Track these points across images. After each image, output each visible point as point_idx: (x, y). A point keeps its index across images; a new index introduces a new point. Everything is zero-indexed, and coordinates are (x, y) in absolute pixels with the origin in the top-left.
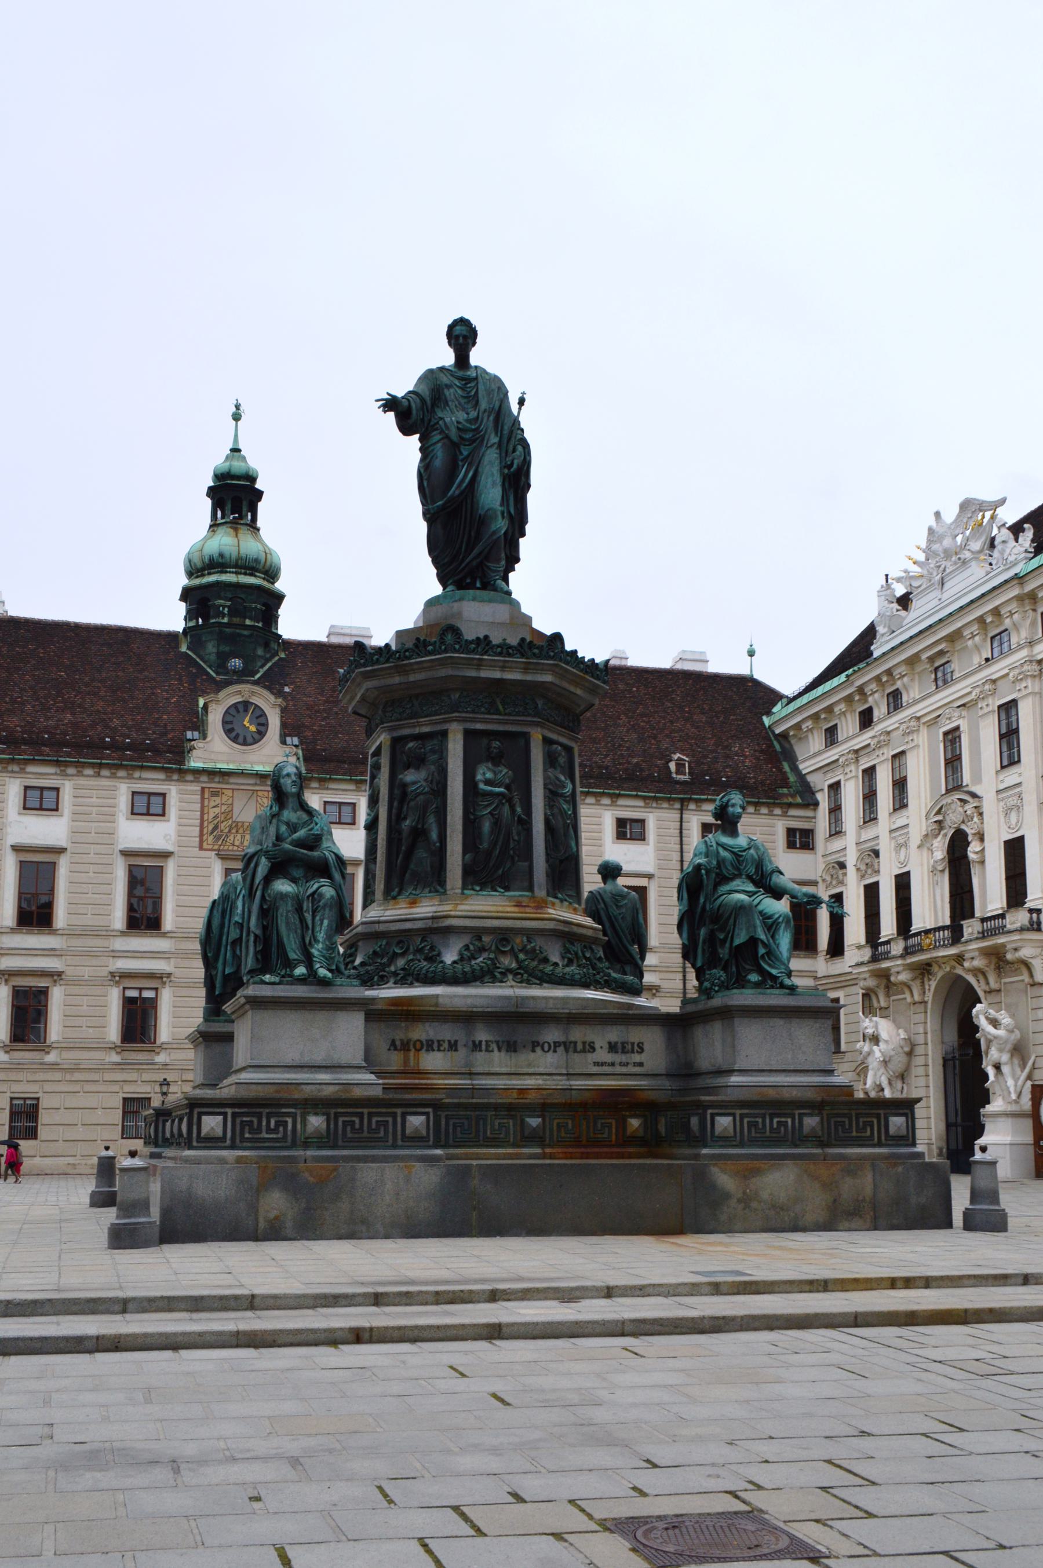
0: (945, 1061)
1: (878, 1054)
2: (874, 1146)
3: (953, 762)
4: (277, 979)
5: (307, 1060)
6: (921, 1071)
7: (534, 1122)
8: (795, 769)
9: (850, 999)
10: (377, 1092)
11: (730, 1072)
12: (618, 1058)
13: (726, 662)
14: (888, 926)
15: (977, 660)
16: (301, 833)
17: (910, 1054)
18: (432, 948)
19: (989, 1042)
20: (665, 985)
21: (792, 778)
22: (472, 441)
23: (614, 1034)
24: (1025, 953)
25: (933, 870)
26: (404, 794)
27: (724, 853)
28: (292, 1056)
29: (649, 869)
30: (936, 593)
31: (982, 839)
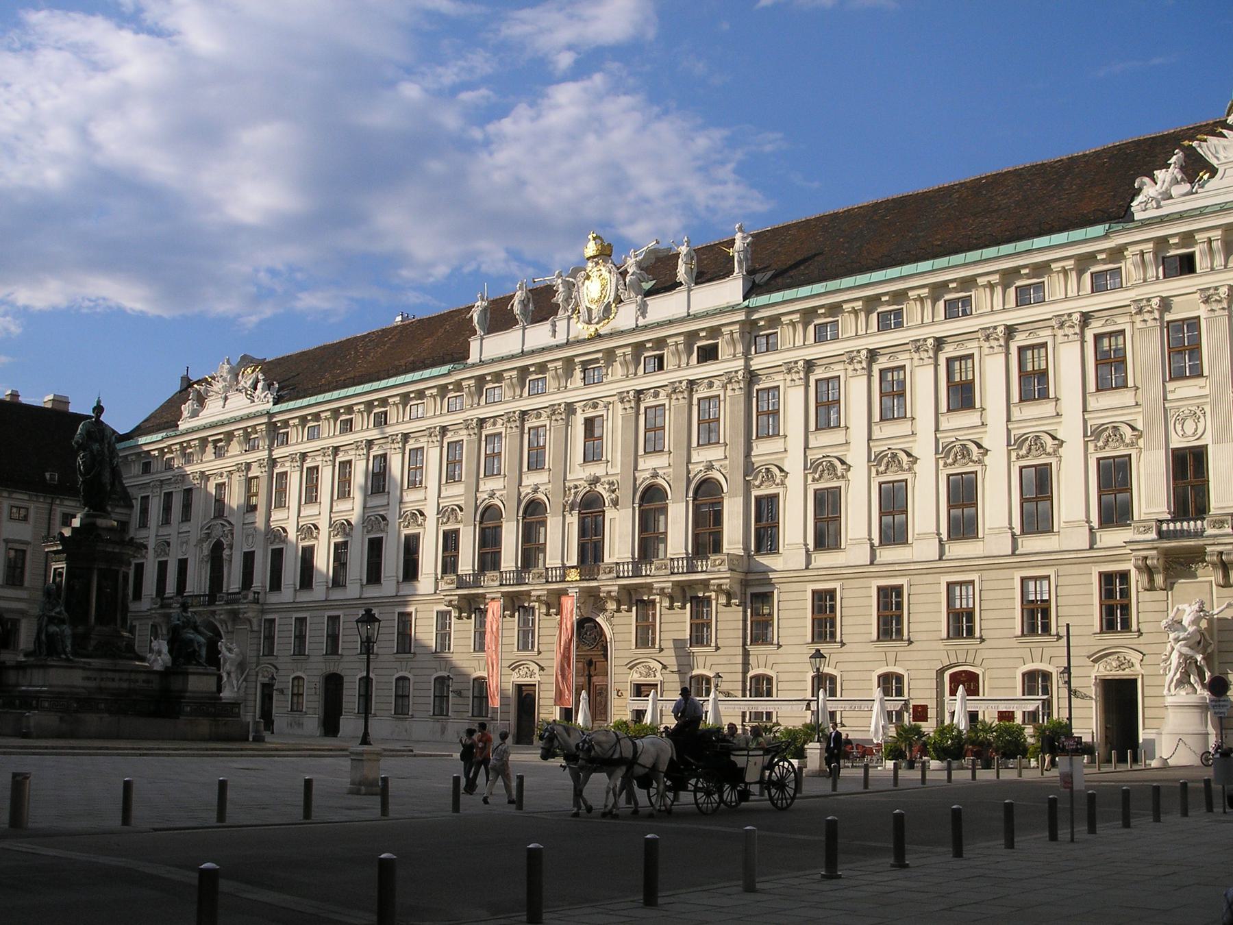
13: (80, 406)
14: (171, 588)
16: (58, 610)
19: (225, 662)
24: (250, 615)
25: (202, 561)
31: (231, 548)
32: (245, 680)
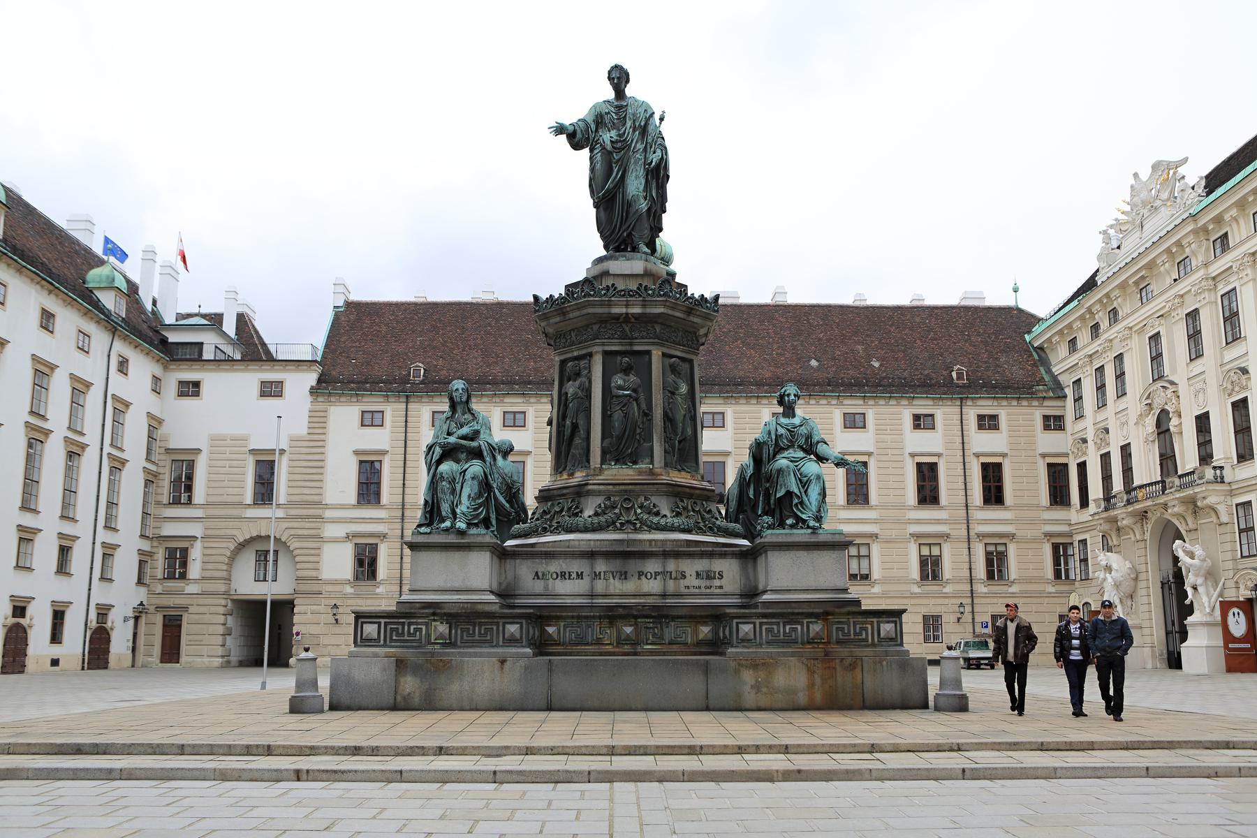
0: (1163, 584)
1: (1110, 580)
2: (868, 646)
3: (1157, 358)
4: (428, 530)
5: (449, 585)
6: (1144, 592)
7: (628, 630)
8: (1049, 371)
9: (1094, 541)
10: (495, 608)
11: (765, 592)
12: (703, 583)
13: (997, 297)
15: (1169, 281)
16: (465, 430)
17: (1136, 579)
18: (577, 507)
20: (953, 533)
21: (1047, 378)
22: (621, 149)
23: (701, 565)
24: (1211, 500)
26: (566, 399)
27: (781, 431)
28: (438, 582)
29: (939, 449)
30: (1138, 234)
31: (1180, 416)
32: (1221, 595)
